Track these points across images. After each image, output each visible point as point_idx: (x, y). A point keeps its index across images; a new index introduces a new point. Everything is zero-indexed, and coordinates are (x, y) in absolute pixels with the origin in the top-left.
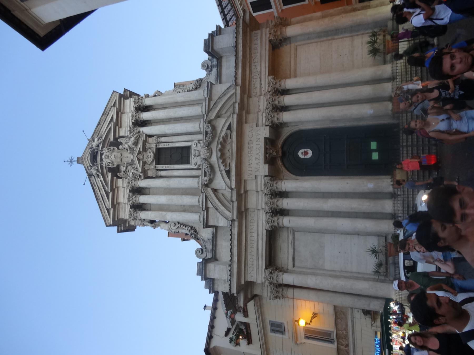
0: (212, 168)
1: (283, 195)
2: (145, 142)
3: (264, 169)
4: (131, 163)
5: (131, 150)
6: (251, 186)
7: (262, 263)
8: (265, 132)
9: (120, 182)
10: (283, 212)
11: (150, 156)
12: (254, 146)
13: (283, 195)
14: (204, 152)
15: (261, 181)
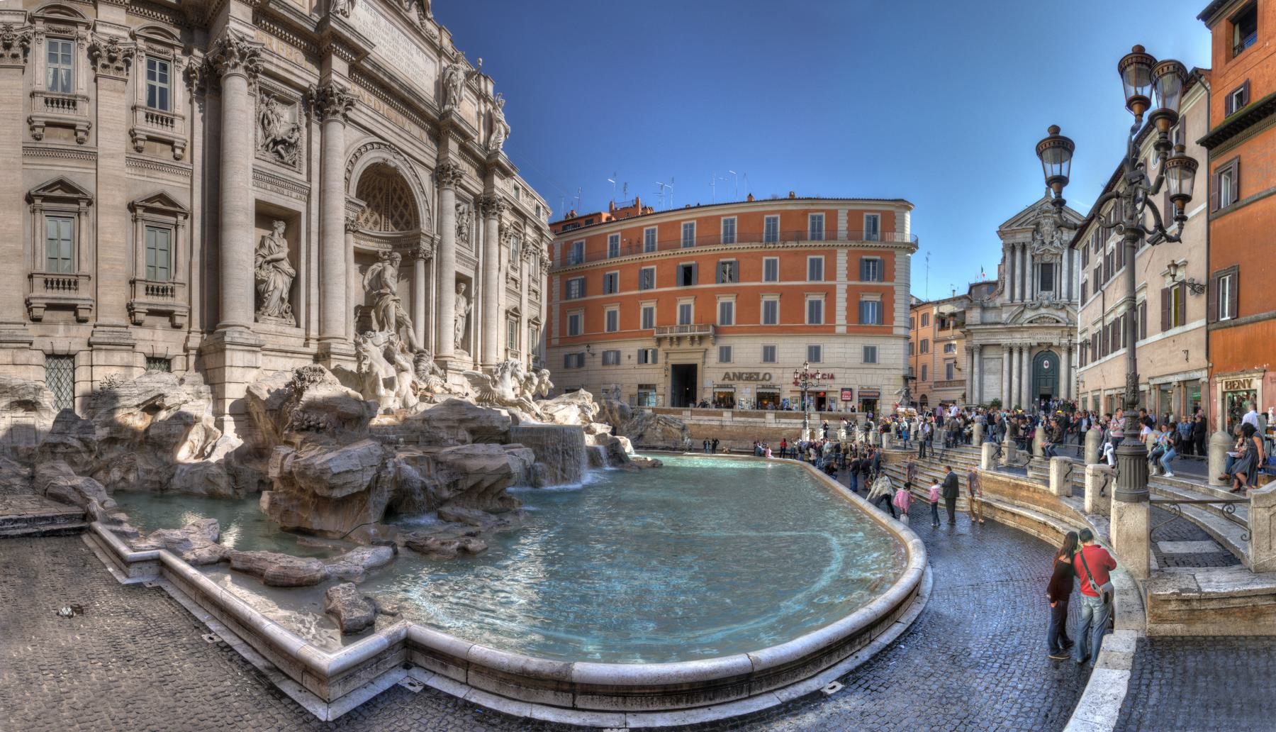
0: (1037, 308)
1: (1021, 353)
2: (1056, 254)
3: (1034, 343)
4: (1043, 243)
5: (1051, 243)
6: (1026, 335)
7: (984, 342)
8: (1055, 343)
9: (1029, 235)
10: (1011, 352)
11: (1047, 259)
12: (1048, 336)
13: (1021, 353)
14: (1046, 302)
15: (1028, 341)
